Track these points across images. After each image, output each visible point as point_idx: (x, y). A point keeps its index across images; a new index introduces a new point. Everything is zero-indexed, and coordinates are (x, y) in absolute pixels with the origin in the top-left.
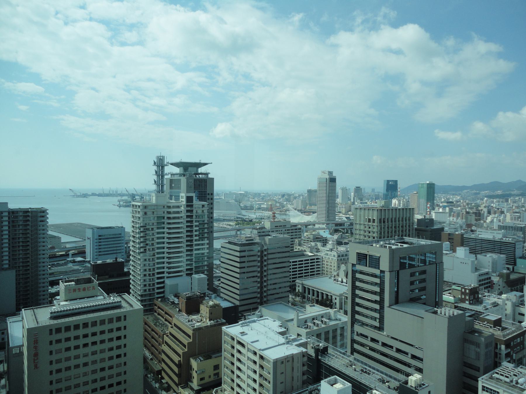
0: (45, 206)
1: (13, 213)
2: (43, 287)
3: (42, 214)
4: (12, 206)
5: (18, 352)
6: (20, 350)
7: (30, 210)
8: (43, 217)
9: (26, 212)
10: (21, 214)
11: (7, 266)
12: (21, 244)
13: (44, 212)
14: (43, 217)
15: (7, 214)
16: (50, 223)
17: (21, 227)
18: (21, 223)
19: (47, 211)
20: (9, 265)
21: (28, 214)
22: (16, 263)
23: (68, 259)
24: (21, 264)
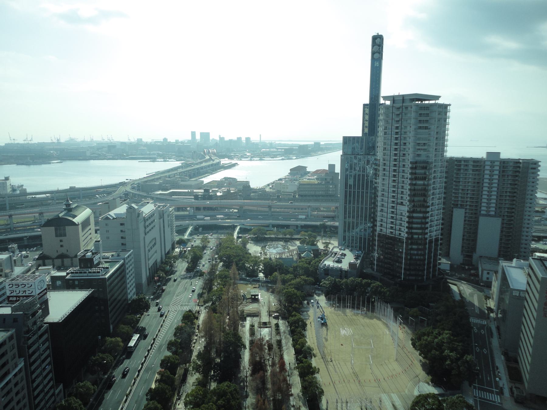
0: (536, 158)
1: (505, 163)
2: (526, 240)
3: (534, 166)
4: (503, 156)
5: (518, 295)
6: (520, 294)
7: (521, 161)
8: (534, 169)
9: (516, 163)
10: (511, 164)
11: (493, 213)
12: (508, 194)
13: (535, 164)
14: (534, 169)
15: (498, 163)
16: (540, 177)
17: (510, 178)
18: (510, 173)
19: (540, 164)
20: (495, 212)
21: (518, 165)
22: (501, 211)
23: (544, 217)
24: (506, 214)
